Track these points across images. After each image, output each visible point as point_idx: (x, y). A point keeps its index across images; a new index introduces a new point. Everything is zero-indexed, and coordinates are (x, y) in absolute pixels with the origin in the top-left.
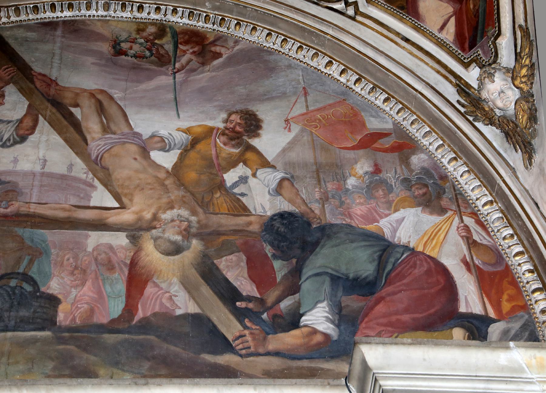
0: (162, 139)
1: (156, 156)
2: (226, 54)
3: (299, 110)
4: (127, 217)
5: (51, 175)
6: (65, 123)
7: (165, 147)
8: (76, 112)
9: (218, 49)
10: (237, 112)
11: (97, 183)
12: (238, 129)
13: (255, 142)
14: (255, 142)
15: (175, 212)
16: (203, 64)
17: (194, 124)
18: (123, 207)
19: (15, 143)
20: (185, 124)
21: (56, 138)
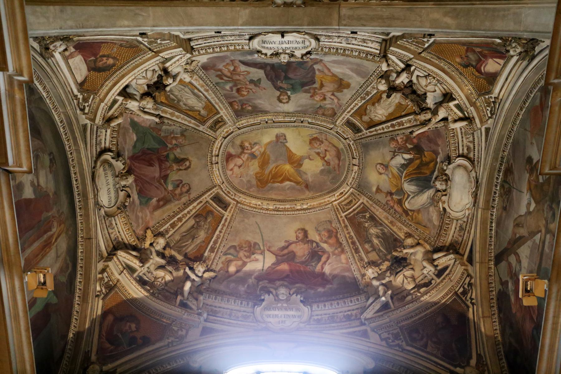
0: (528, 203)
1: (531, 209)
2: (512, 161)
3: (529, 134)
4: (543, 231)
5: (530, 255)
6: (519, 242)
7: (529, 204)
8: (518, 236)
9: (510, 164)
10: (526, 166)
11: (534, 238)
12: (530, 168)
13: (535, 161)
14: (535, 161)
15: (545, 209)
16: (513, 173)
17: (526, 187)
18: (540, 231)
19: (520, 265)
20: (525, 192)
21: (522, 247)
